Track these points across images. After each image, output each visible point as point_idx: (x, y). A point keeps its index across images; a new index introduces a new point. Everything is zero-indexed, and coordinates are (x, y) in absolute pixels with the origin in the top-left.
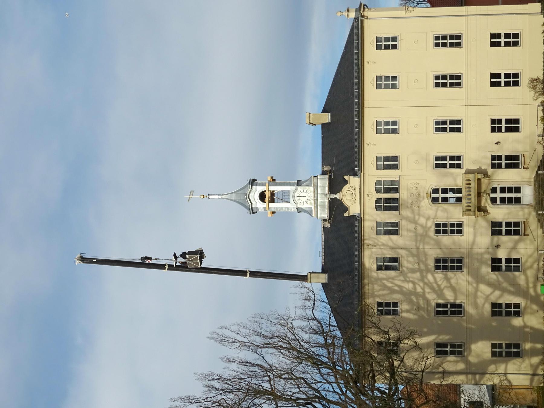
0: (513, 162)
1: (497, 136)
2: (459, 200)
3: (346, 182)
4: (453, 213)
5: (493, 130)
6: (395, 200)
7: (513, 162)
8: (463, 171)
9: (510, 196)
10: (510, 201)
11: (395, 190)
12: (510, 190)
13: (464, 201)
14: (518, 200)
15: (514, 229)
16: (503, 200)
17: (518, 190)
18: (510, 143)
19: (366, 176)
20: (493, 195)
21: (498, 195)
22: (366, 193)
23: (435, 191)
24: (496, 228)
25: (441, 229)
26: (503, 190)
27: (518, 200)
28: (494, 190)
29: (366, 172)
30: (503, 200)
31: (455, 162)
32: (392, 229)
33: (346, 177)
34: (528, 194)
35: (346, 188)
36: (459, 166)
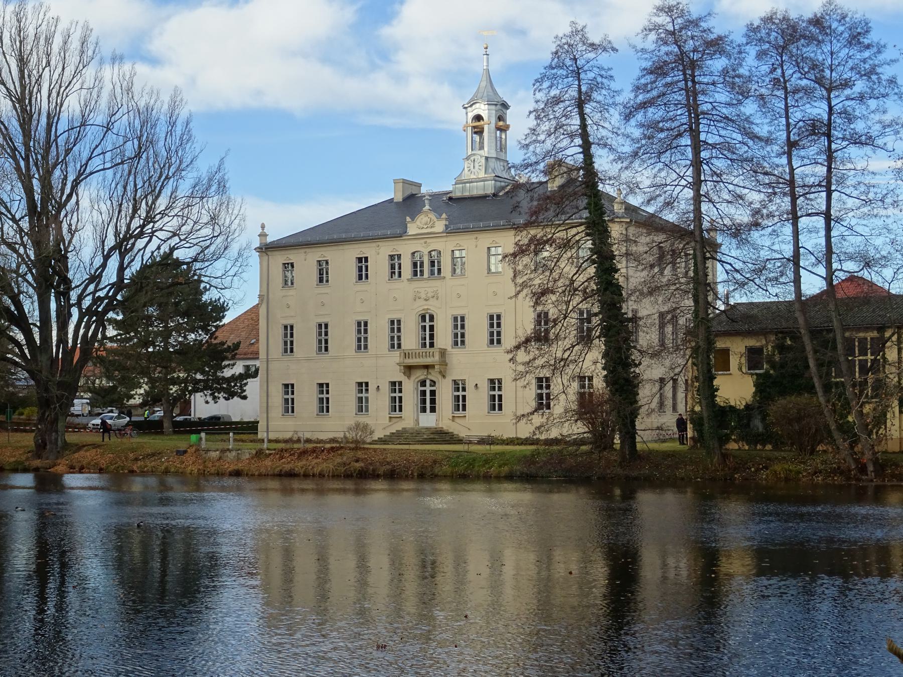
0: (460, 404)
1: (485, 386)
2: (424, 345)
3: (439, 217)
4: (410, 339)
5: (492, 381)
6: (422, 272)
7: (460, 404)
8: (449, 348)
9: (428, 402)
10: (424, 401)
11: (432, 273)
12: (433, 401)
13: (424, 350)
14: (424, 410)
15: (396, 405)
16: (423, 393)
17: (433, 410)
18: (478, 400)
19: (445, 239)
20: (428, 383)
21: (428, 389)
22: (428, 241)
23: (432, 318)
24: (395, 386)
25: (395, 326)
26: (433, 393)
27: (424, 410)
28: (433, 383)
29: (449, 239)
30: (423, 393)
31: (459, 339)
32: (395, 270)
33: (444, 216)
34: (428, 421)
35: (432, 216)
36: (456, 343)
